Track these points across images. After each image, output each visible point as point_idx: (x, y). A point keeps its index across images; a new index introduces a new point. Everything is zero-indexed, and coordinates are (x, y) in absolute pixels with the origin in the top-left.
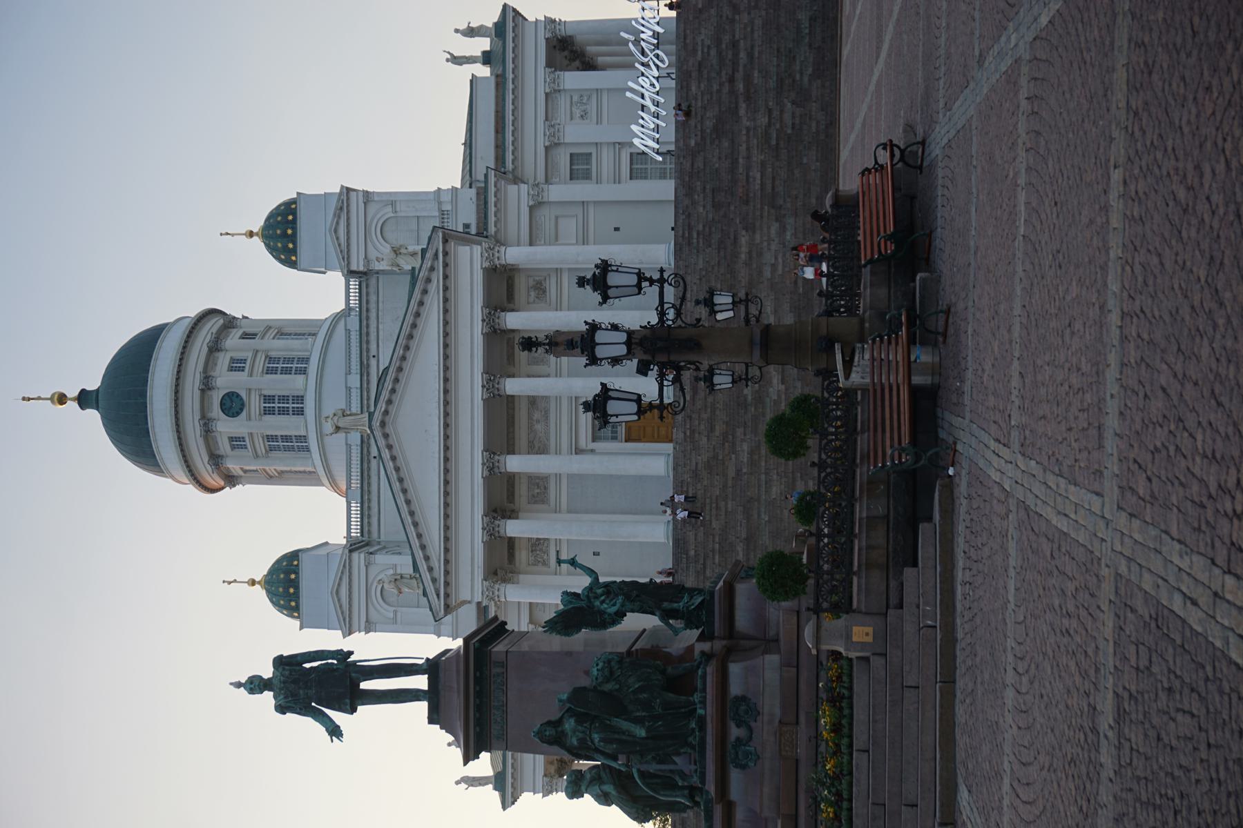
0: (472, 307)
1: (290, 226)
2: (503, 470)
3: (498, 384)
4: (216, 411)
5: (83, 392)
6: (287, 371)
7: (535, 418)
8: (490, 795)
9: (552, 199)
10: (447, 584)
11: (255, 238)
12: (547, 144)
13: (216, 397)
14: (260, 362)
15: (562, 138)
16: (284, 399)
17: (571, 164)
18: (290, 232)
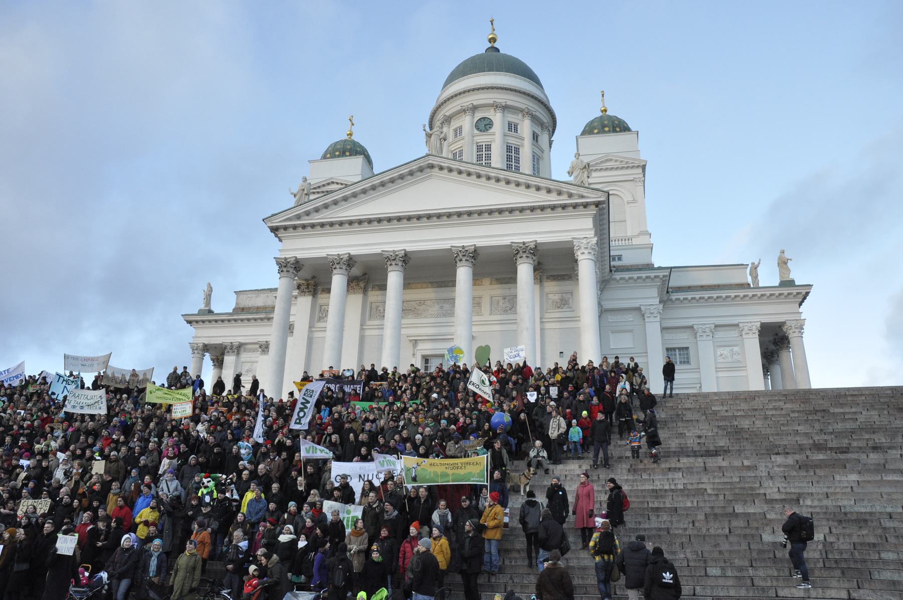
0: (536, 233)
1: (611, 129)
2: (389, 270)
3: (466, 260)
4: (479, 115)
5: (497, 50)
6: (509, 158)
7: (444, 305)
8: (195, 305)
9: (646, 324)
10: (295, 227)
11: (601, 114)
12: (695, 327)
13: (490, 114)
14: (512, 141)
15: (701, 338)
16: (489, 157)
17: (680, 349)
18: (607, 129)
